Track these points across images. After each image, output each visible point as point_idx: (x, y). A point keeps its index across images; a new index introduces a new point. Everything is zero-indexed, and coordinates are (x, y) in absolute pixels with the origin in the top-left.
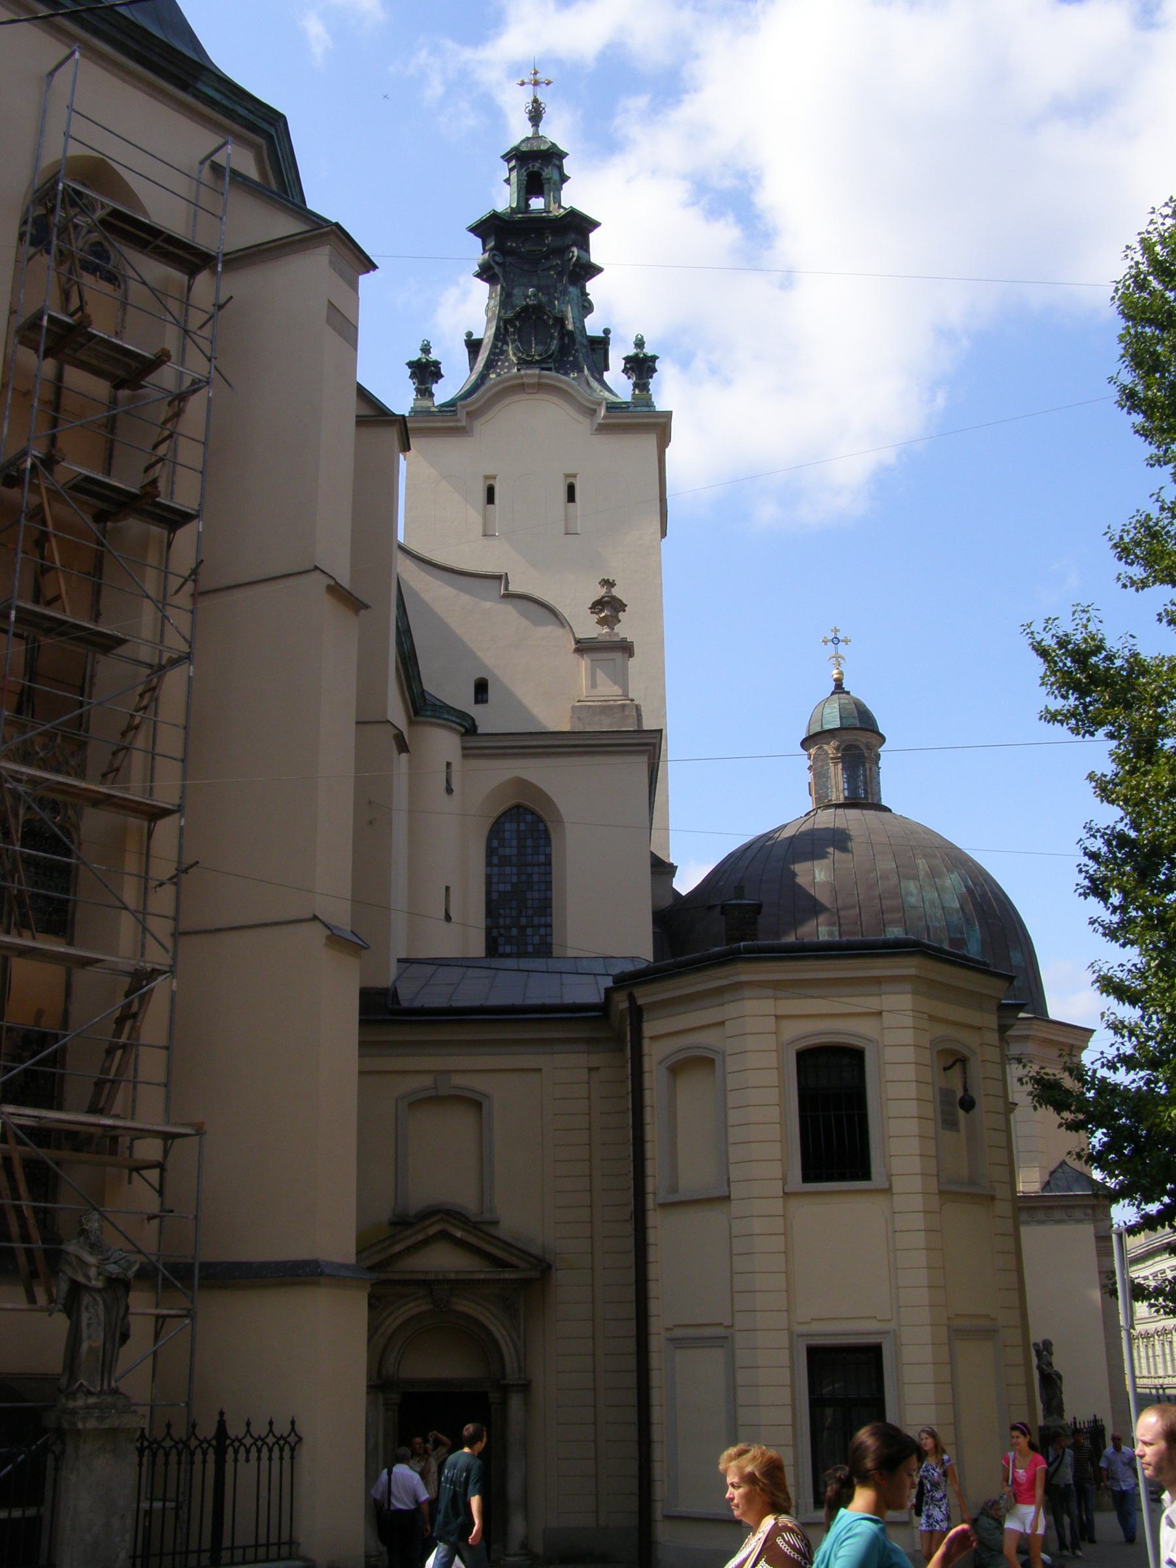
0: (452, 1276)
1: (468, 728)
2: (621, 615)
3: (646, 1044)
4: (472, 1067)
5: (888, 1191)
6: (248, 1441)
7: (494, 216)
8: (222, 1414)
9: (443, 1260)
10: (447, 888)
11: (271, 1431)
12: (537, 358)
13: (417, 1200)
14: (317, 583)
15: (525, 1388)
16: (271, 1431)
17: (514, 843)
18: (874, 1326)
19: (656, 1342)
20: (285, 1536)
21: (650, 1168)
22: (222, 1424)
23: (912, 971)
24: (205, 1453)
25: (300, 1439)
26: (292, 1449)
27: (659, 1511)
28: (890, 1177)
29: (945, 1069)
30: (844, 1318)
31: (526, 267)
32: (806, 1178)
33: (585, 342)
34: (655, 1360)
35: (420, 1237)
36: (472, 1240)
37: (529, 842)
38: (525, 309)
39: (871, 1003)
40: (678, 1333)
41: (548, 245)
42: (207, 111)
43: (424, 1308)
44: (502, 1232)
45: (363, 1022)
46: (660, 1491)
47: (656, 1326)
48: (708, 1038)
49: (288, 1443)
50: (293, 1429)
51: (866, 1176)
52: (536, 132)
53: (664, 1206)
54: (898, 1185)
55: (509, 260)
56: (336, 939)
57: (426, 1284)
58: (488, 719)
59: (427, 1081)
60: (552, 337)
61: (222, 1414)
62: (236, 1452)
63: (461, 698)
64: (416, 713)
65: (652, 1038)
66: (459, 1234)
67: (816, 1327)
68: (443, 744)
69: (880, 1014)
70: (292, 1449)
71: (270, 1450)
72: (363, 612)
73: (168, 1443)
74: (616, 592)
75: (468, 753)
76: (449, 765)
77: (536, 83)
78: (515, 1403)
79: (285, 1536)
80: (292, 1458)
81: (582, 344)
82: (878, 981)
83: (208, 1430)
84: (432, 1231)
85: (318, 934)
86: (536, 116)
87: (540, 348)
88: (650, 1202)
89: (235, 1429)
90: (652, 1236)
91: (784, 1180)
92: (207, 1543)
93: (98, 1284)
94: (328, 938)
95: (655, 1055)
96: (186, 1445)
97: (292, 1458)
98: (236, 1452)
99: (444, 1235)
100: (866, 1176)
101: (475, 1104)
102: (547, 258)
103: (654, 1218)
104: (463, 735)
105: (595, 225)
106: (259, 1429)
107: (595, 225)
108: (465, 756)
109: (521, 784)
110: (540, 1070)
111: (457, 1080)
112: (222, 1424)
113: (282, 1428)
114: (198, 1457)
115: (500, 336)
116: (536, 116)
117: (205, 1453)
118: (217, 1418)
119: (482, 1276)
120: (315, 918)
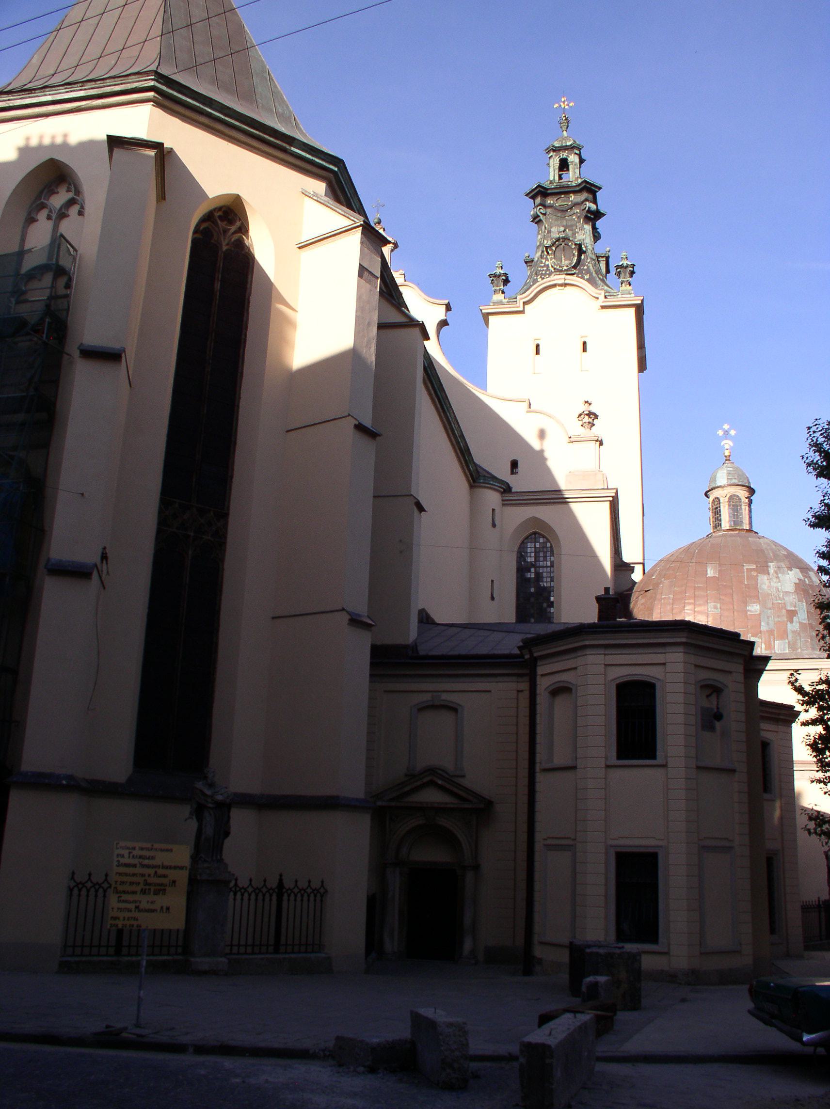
1: (506, 489)
2: (596, 421)
3: (538, 677)
4: (452, 689)
8: (281, 875)
9: (432, 796)
10: (492, 581)
11: (309, 886)
12: (565, 268)
15: (476, 868)
16: (309, 886)
17: (533, 555)
18: (653, 842)
19: (538, 847)
21: (539, 748)
22: (281, 881)
23: (683, 640)
24: (271, 895)
25: (326, 891)
26: (322, 896)
27: (536, 939)
28: (666, 757)
29: (708, 696)
30: (637, 837)
31: (559, 215)
32: (619, 757)
34: (537, 857)
35: (419, 783)
36: (448, 786)
37: (541, 554)
38: (558, 240)
39: (660, 658)
40: (549, 842)
44: (465, 782)
45: (373, 665)
46: (537, 928)
47: (539, 837)
48: (565, 677)
49: (320, 893)
50: (322, 886)
51: (654, 757)
55: (549, 211)
56: (355, 622)
57: (422, 809)
58: (518, 484)
59: (426, 697)
60: (574, 255)
61: (281, 875)
62: (289, 896)
63: (502, 472)
64: (474, 481)
65: (542, 675)
66: (440, 782)
67: (621, 842)
68: (491, 498)
69: (664, 664)
70: (322, 896)
71: (309, 896)
72: (378, 438)
74: (593, 409)
75: (505, 503)
76: (493, 510)
78: (470, 876)
80: (322, 901)
81: (591, 259)
82: (664, 645)
83: (273, 883)
84: (425, 780)
87: (567, 262)
88: (538, 767)
89: (288, 883)
90: (539, 787)
91: (606, 758)
92: (272, 942)
93: (211, 805)
94: (350, 620)
95: (543, 684)
96: (260, 890)
97: (322, 901)
98: (289, 896)
99: (432, 783)
100: (654, 757)
101: (453, 709)
102: (571, 209)
103: (539, 777)
104: (502, 493)
106: (302, 884)
108: (503, 505)
109: (535, 520)
110: (490, 691)
111: (444, 696)
112: (281, 881)
113: (316, 884)
117: (271, 895)
118: (278, 877)
119: (452, 806)
120: (343, 609)
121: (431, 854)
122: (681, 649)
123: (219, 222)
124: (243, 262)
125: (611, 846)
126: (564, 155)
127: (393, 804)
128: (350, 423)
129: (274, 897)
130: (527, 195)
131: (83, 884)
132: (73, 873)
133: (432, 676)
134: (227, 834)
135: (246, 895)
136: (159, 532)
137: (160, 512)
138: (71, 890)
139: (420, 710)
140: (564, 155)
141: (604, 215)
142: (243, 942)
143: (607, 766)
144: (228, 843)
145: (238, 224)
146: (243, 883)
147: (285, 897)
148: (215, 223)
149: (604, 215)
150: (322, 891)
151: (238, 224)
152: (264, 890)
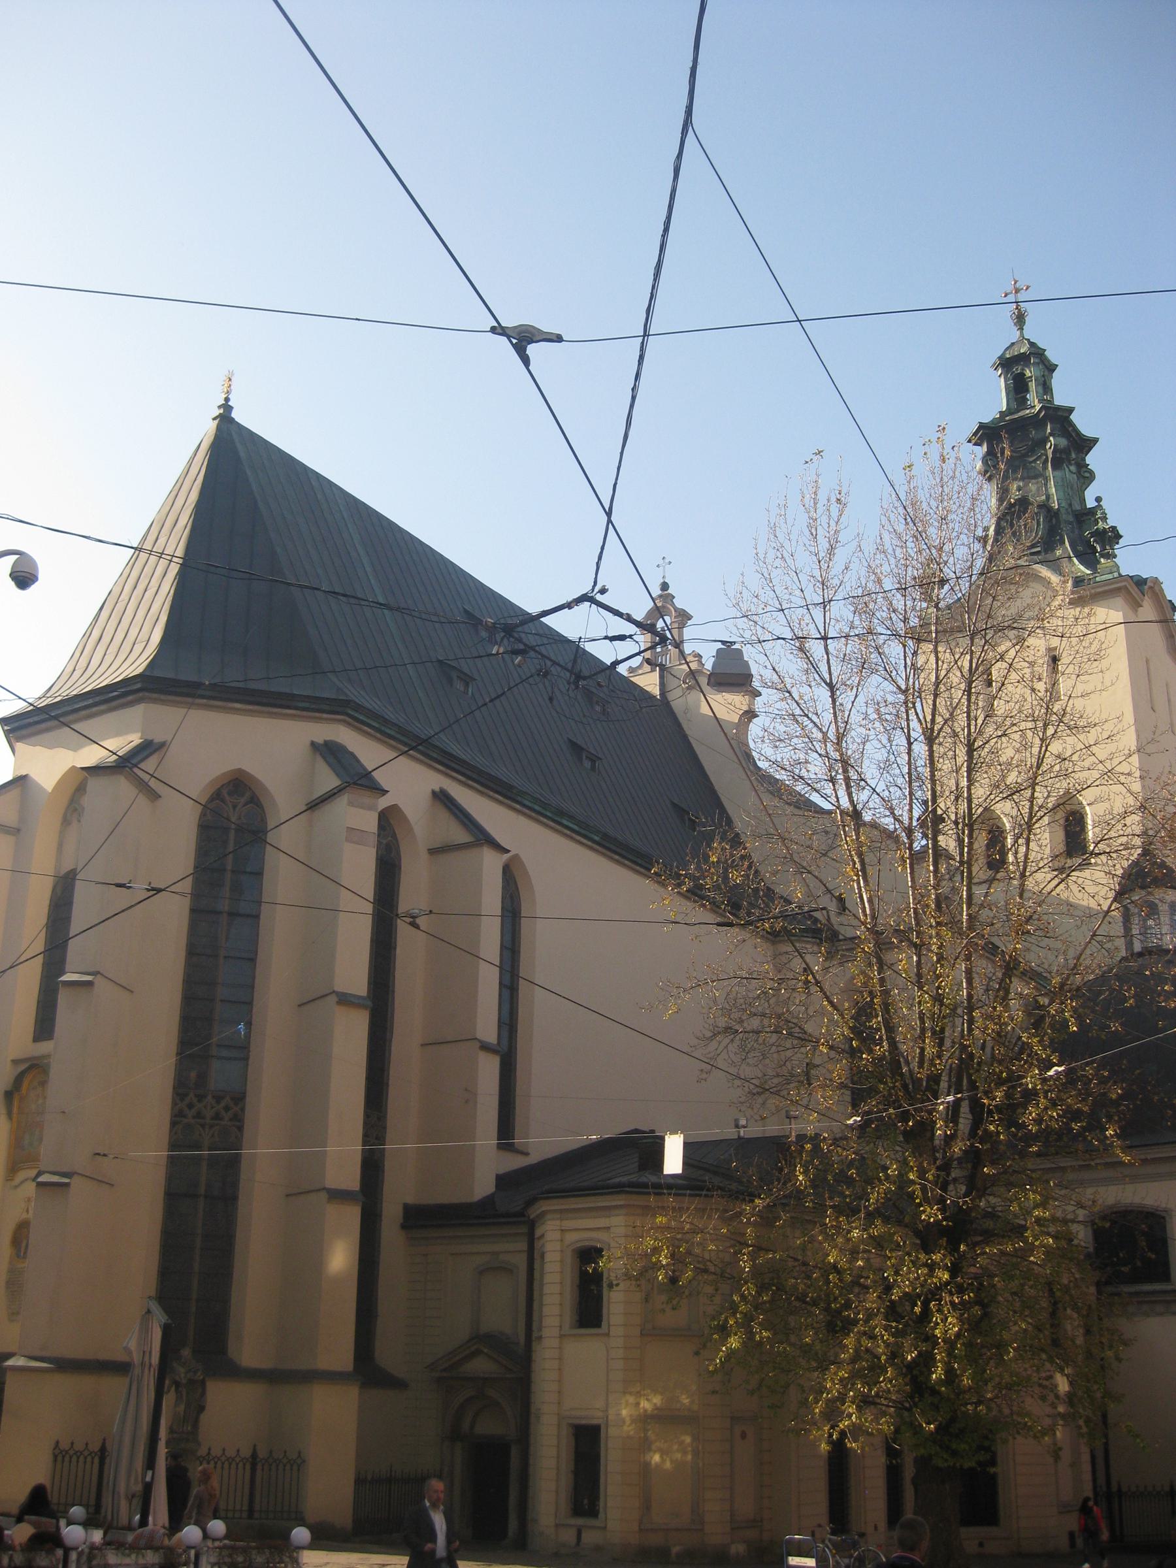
5: (608, 1335)
6: (285, 1461)
7: (982, 426)
9: (481, 1366)
14: (333, 999)
23: (622, 1203)
26: (299, 1466)
33: (1071, 518)
39: (602, 1222)
41: (1033, 439)
49: (298, 1463)
50: (299, 1456)
52: (1022, 334)
53: (121, 1368)
77: (1017, 291)
84: (473, 1349)
86: (1020, 319)
89: (262, 1454)
92: (245, 1508)
99: (477, 1353)
105: (1071, 410)
107: (1071, 410)
115: (999, 531)
116: (1020, 319)
121: (488, 1427)
123: (227, 797)
124: (255, 833)
126: (1017, 369)
128: (334, 998)
130: (969, 441)
131: (67, 1452)
132: (57, 1442)
134: (202, 1409)
136: (173, 1124)
137: (174, 1104)
138: (55, 1457)
139: (481, 1273)
140: (1017, 369)
141: (1095, 441)
142: (238, 1507)
144: (204, 1418)
145: (248, 794)
147: (259, 1467)
148: (223, 801)
149: (1095, 441)
150: (299, 1461)
151: (248, 794)
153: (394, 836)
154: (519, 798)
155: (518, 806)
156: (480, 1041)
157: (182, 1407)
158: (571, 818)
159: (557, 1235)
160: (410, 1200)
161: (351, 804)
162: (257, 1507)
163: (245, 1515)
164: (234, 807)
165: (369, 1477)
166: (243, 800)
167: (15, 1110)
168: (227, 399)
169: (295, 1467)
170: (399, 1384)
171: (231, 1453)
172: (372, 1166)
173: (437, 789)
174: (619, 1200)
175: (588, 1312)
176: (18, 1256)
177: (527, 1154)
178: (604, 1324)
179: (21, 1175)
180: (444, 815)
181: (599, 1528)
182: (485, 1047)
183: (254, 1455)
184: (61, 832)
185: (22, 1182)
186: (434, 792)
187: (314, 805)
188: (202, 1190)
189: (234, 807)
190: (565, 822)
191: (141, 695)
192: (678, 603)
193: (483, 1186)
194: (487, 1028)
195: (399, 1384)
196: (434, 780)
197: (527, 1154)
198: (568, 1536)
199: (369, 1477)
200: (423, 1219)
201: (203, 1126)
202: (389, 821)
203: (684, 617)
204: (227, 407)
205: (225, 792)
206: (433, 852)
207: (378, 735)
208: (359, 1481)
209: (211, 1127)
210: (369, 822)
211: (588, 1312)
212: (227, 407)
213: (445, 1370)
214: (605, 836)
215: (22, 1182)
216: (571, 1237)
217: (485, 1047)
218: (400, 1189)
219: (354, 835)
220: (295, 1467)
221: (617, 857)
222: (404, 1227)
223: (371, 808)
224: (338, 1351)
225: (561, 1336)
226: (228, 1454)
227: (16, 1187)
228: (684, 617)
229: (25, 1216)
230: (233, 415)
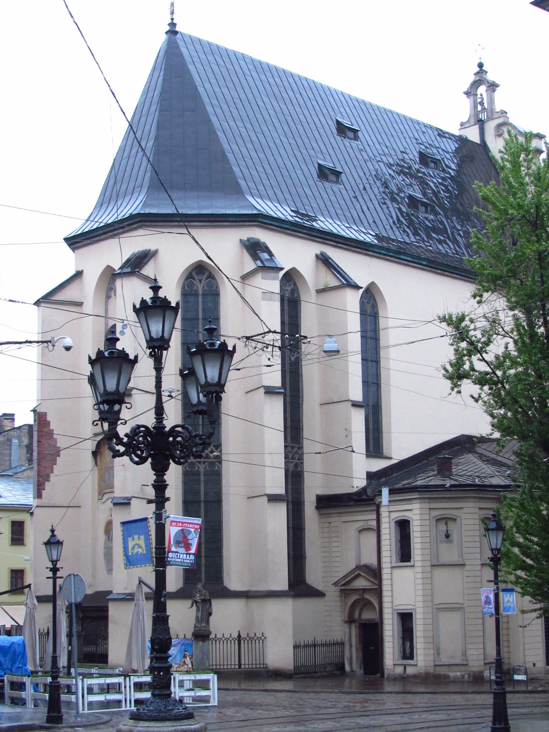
0: (361, 587)
8: (239, 632)
9: (361, 583)
13: (363, 562)
18: (411, 607)
20: (262, 662)
23: (417, 496)
26: (263, 641)
42: (234, 224)
43: (358, 597)
49: (262, 639)
54: (418, 564)
59: (361, 524)
61: (239, 632)
70: (263, 641)
73: (231, 639)
79: (262, 662)
83: (235, 635)
84: (356, 573)
85: (265, 499)
89: (243, 635)
92: (237, 663)
93: (200, 601)
99: (359, 576)
114: (233, 642)
119: (368, 587)
121: (368, 615)
122: (418, 501)
123: (196, 277)
124: (213, 295)
125: (395, 610)
127: (342, 588)
128: (262, 390)
129: (237, 642)
133: (367, 511)
134: (210, 614)
135: (261, 641)
139: (360, 531)
143: (392, 567)
146: (219, 636)
147: (242, 642)
148: (194, 279)
150: (263, 638)
152: (223, 639)
153: (295, 284)
154: (372, 249)
155: (371, 253)
156: (351, 401)
157: (200, 614)
158: (405, 254)
159: (387, 514)
160: (320, 492)
161: (263, 278)
162: (243, 663)
163: (237, 667)
164: (200, 281)
165: (302, 644)
166: (205, 277)
167: (98, 461)
168: (172, 19)
169: (261, 641)
170: (319, 594)
171: (227, 636)
172: (294, 476)
173: (319, 253)
174: (415, 495)
175: (405, 554)
176: (109, 540)
177: (390, 458)
178: (412, 560)
179: (106, 497)
180: (323, 269)
181: (415, 665)
182: (355, 405)
183: (239, 636)
184: (106, 302)
185: (107, 500)
186: (317, 256)
187: (245, 278)
188: (202, 498)
189: (200, 281)
190: (402, 257)
191: (140, 224)
192: (490, 77)
193: (359, 482)
194: (356, 392)
195: (319, 594)
196: (316, 248)
197: (390, 458)
198: (399, 670)
199: (302, 644)
200: (326, 503)
201: (200, 463)
202: (291, 279)
203: (493, 86)
204: (173, 25)
205: (194, 274)
206: (319, 291)
207: (279, 229)
208: (296, 647)
209: (204, 463)
210: (273, 285)
211: (405, 554)
212: (173, 25)
213: (344, 585)
214: (429, 261)
215: (107, 500)
216: (394, 515)
217: (355, 405)
218: (313, 487)
219: (267, 295)
220: (261, 641)
221: (439, 271)
222: (317, 508)
223: (274, 279)
224: (280, 581)
225: (392, 567)
226: (226, 636)
227: (104, 503)
228: (493, 86)
229: (110, 518)
230: (178, 29)
